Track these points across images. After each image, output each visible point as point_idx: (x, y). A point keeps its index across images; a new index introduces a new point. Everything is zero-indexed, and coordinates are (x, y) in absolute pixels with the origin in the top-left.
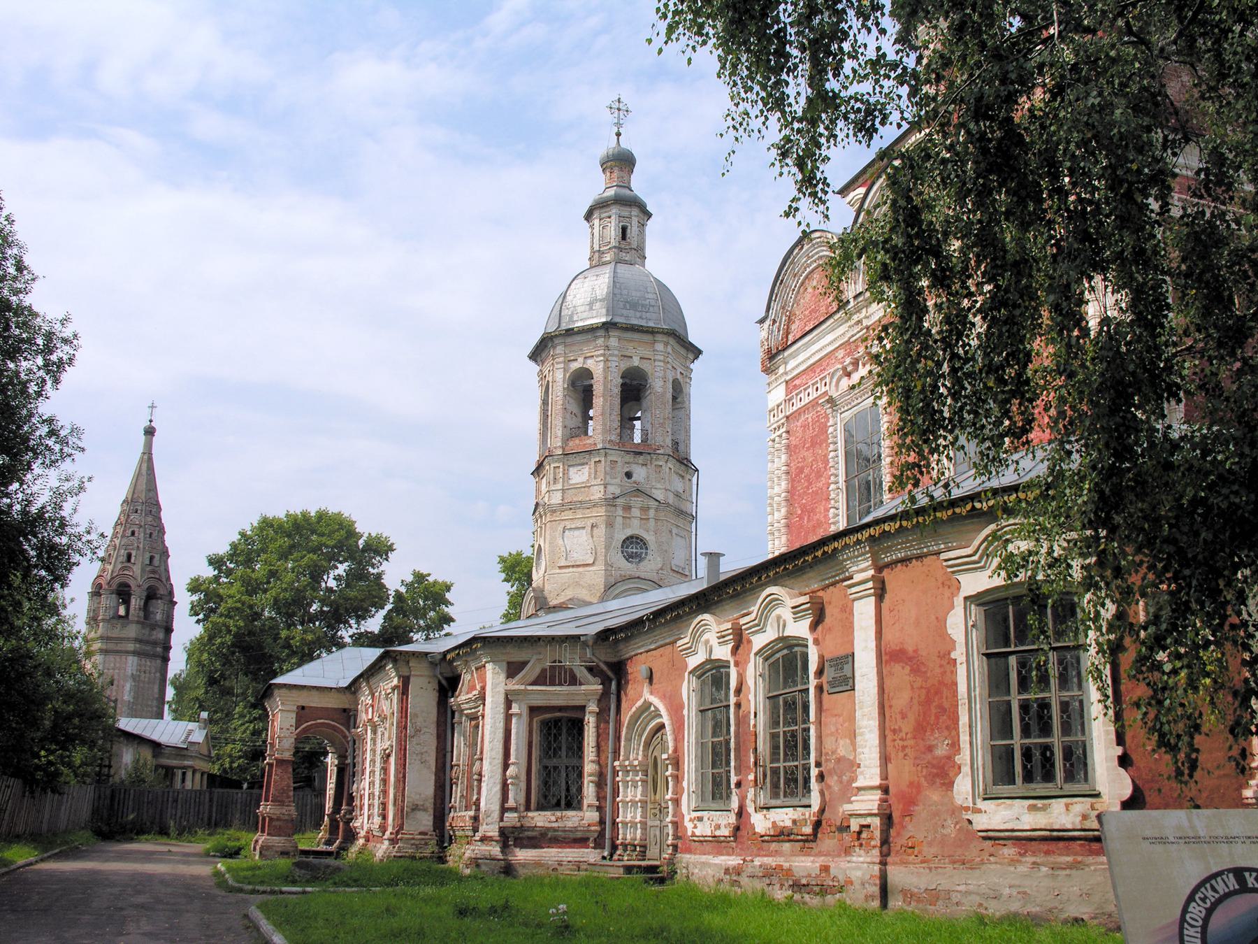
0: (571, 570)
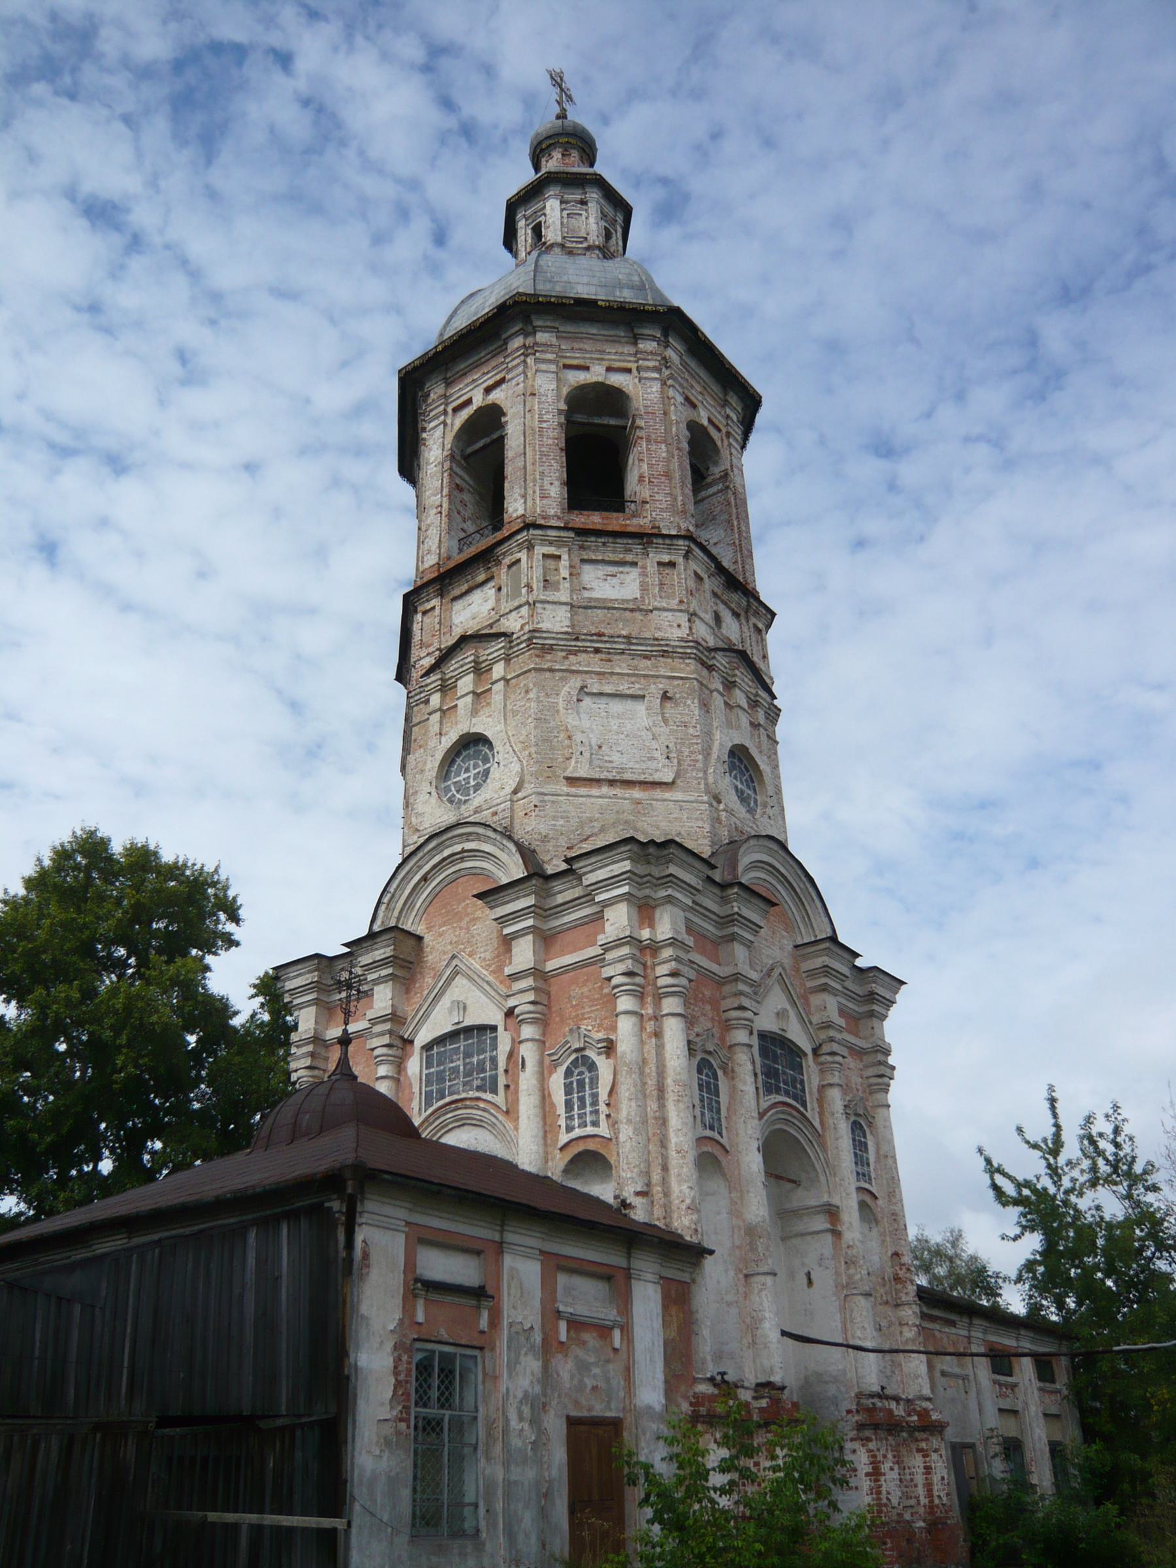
0: (605, 790)
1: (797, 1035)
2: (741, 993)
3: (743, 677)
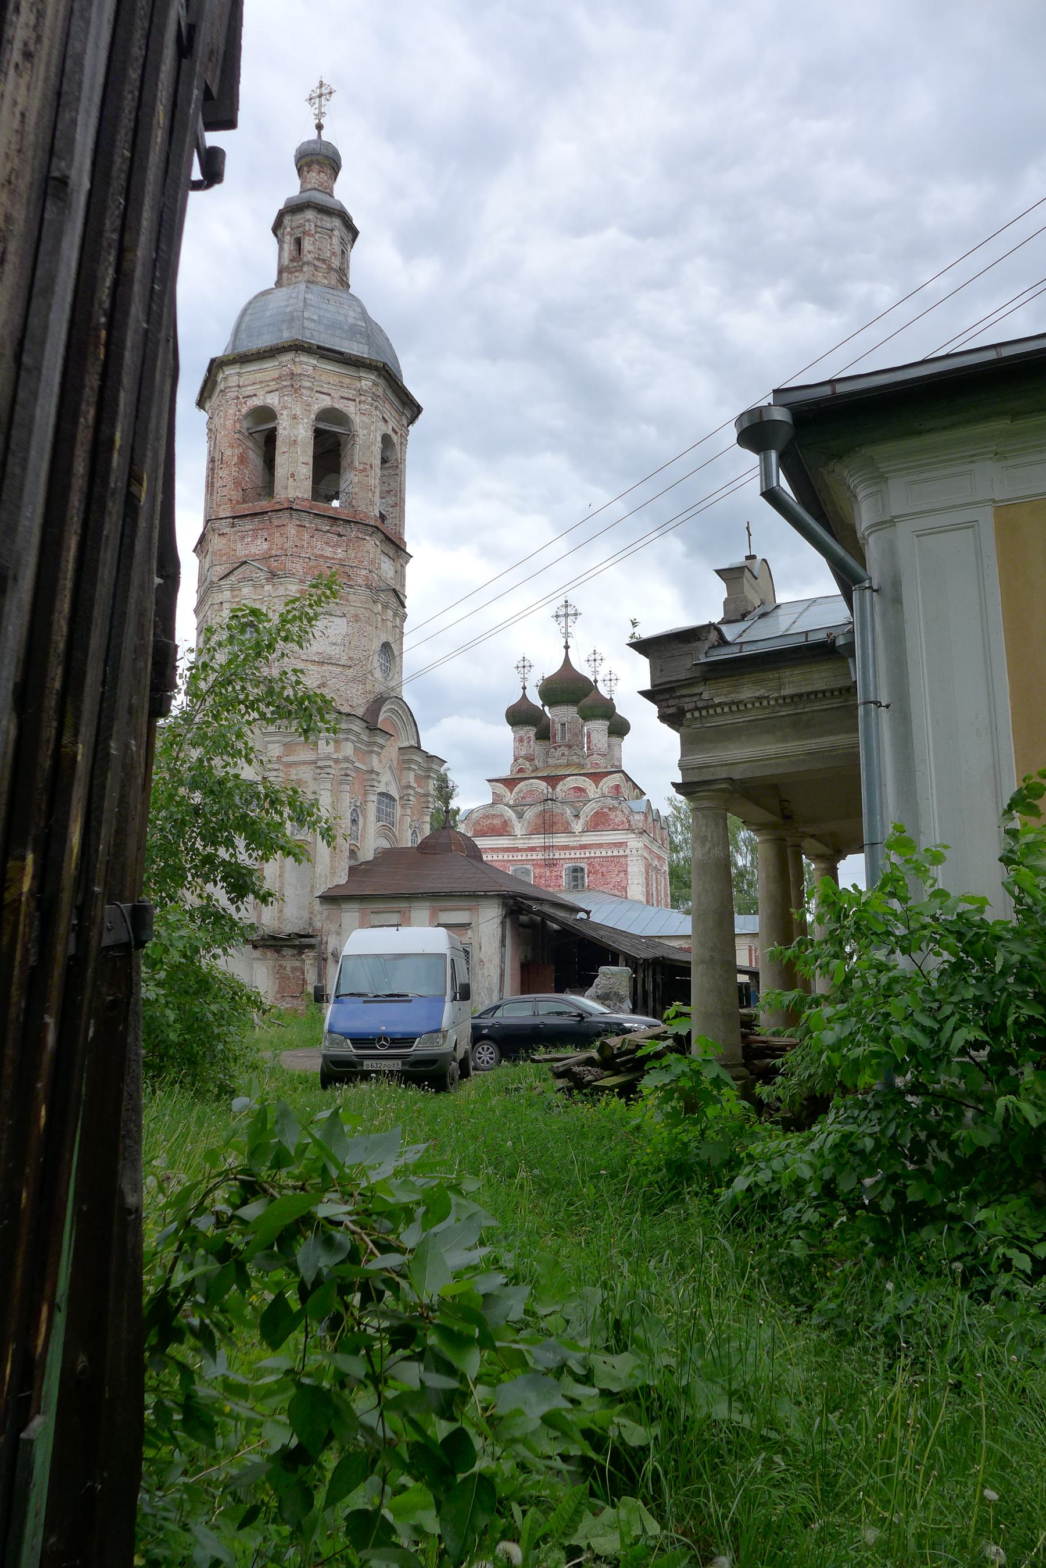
1: (394, 793)
2: (373, 779)
3: (393, 600)
